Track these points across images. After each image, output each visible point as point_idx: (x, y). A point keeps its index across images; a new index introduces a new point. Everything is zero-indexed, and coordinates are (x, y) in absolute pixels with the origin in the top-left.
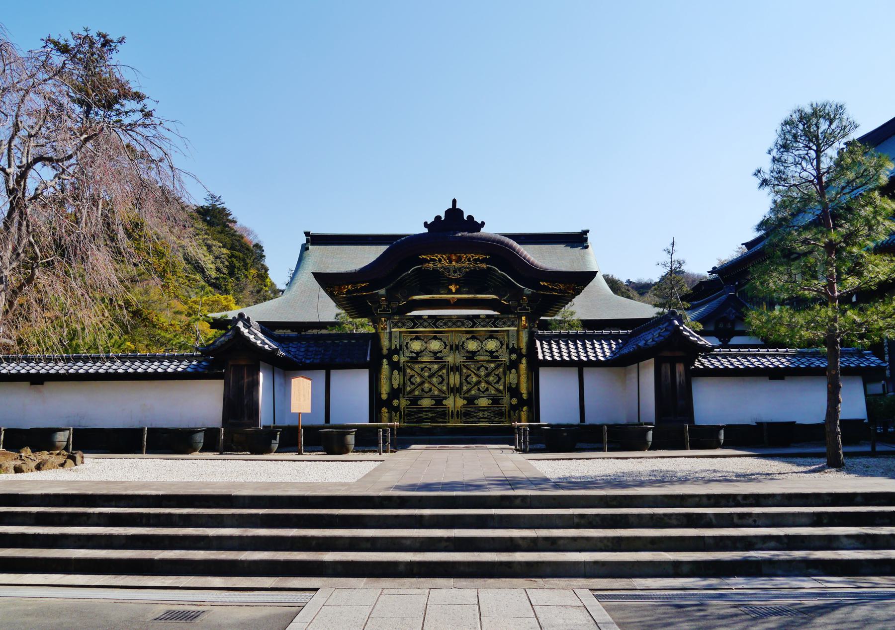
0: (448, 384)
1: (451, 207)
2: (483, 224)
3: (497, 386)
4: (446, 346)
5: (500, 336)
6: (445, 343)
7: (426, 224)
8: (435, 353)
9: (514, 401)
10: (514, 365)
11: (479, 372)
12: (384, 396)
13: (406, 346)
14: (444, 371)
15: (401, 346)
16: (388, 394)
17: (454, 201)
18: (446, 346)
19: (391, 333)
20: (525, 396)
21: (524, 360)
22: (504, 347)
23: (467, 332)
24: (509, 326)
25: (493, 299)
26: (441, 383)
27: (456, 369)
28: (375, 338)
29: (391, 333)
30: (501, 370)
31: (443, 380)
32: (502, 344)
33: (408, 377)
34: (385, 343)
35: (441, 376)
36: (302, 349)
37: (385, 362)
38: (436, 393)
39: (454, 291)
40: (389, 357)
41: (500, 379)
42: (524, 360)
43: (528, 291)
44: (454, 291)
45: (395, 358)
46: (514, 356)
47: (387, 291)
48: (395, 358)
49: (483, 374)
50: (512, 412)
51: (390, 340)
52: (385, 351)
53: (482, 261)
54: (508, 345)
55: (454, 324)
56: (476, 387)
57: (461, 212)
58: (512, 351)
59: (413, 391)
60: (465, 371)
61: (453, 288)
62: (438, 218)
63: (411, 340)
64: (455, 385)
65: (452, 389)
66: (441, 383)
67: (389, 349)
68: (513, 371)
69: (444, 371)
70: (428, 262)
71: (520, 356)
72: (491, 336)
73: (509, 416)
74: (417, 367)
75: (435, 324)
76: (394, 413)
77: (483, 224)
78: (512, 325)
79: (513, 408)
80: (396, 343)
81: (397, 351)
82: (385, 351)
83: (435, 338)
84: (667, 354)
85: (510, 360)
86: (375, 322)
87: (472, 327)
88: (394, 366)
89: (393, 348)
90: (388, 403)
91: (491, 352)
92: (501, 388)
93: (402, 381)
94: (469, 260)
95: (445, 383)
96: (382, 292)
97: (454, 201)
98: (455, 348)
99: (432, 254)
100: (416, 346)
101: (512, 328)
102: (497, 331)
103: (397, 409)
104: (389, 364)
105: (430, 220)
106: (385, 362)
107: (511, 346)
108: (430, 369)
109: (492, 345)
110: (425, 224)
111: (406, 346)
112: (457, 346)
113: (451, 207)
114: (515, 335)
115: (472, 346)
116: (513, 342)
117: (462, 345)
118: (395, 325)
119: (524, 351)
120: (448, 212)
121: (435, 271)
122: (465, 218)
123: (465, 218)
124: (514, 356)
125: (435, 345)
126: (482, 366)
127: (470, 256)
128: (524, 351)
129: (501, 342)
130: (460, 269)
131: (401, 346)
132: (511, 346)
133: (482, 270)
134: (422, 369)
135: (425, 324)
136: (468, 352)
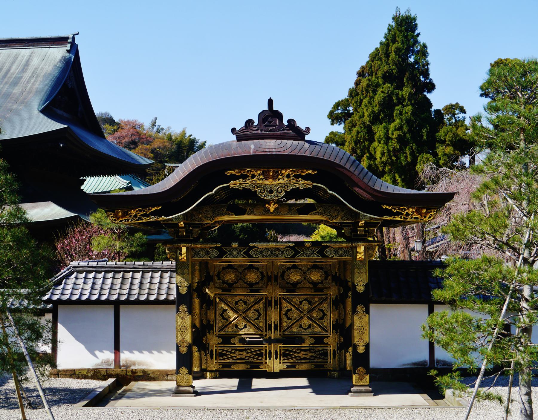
1: (266, 108)
2: (308, 130)
7: (233, 130)
14: (261, 305)
17: (270, 102)
22: (329, 278)
26: (257, 319)
31: (260, 315)
35: (257, 311)
49: (305, 308)
56: (297, 324)
57: (279, 115)
61: (272, 208)
62: (249, 122)
69: (261, 305)
76: (203, 352)
77: (308, 130)
91: (315, 284)
97: (270, 102)
105: (240, 125)
110: (233, 130)
112: (276, 278)
113: (266, 108)
120: (263, 116)
122: (285, 123)
123: (285, 123)
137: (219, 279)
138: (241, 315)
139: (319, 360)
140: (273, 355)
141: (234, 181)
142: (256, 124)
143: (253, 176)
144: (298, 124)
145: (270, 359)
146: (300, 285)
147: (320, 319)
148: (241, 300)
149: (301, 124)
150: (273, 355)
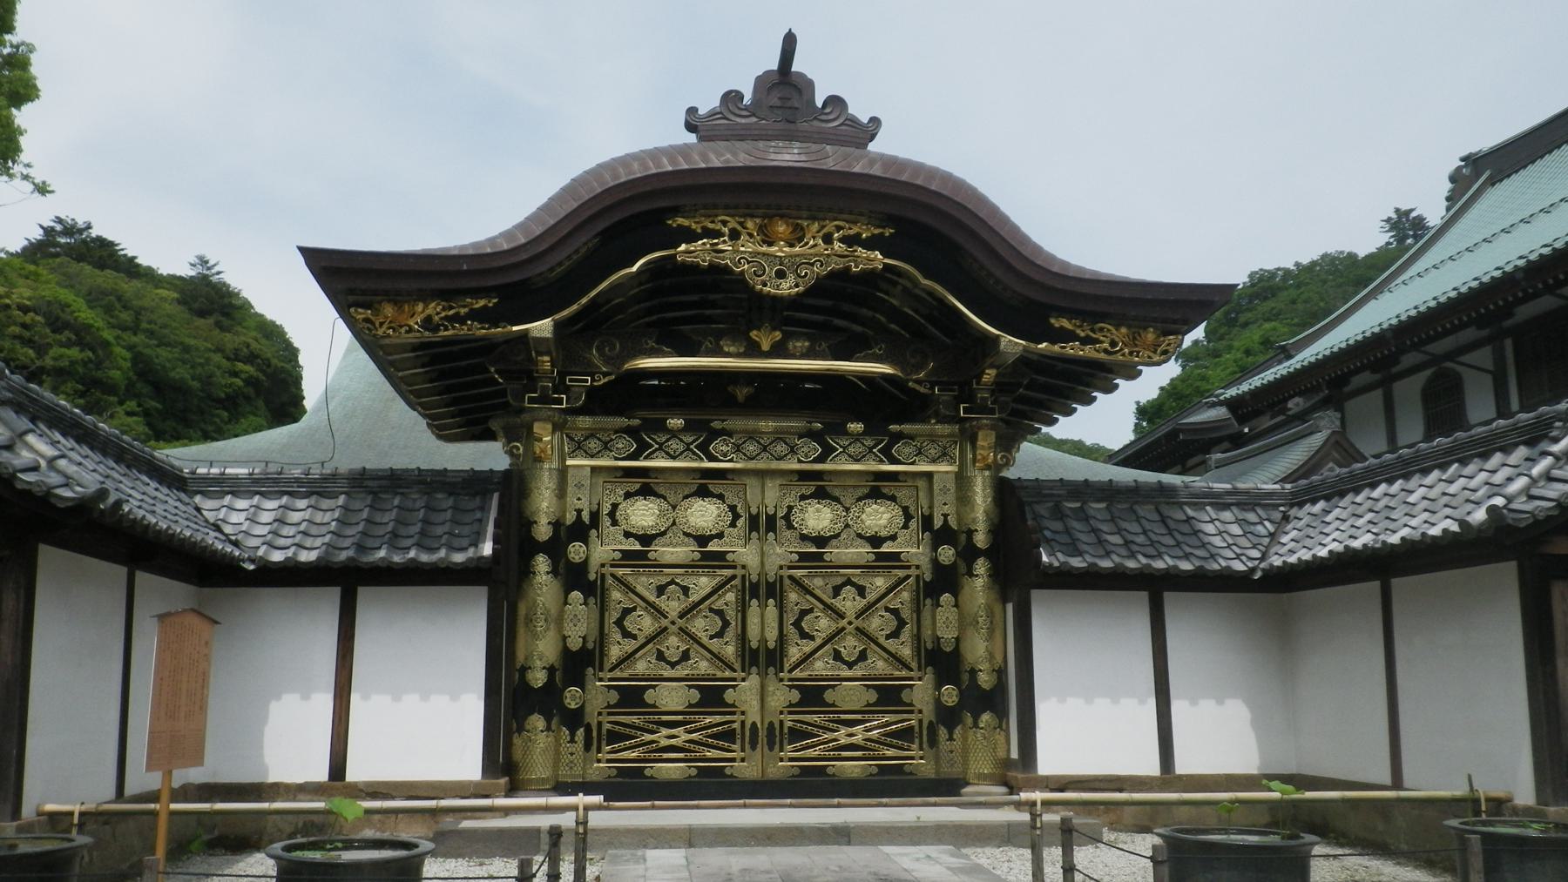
0: (743, 638)
1: (774, 65)
2: (875, 121)
3: (891, 644)
4: (736, 517)
5: (903, 494)
6: (733, 508)
8: (702, 540)
9: (950, 695)
10: (944, 581)
11: (837, 603)
12: (538, 678)
13: (612, 514)
15: (595, 516)
16: (551, 670)
17: (789, 44)
18: (736, 517)
19: (563, 472)
20: (985, 680)
21: (981, 566)
22: (913, 524)
23: (804, 476)
24: (934, 461)
25: (884, 376)
27: (767, 589)
28: (512, 488)
29: (563, 472)
30: (906, 595)
31: (726, 624)
32: (908, 516)
33: (615, 615)
34: (544, 506)
36: (266, 517)
37: (542, 563)
38: (704, 667)
39: (765, 347)
40: (555, 548)
41: (902, 623)
42: (981, 566)
43: (1011, 344)
44: (765, 347)
45: (576, 551)
46: (947, 554)
47: (558, 326)
48: (576, 551)
50: (943, 732)
51: (561, 493)
52: (543, 532)
53: (870, 244)
54: (927, 522)
55: (765, 449)
57: (804, 87)
58: (943, 535)
59: (629, 658)
60: (793, 596)
62: (731, 97)
63: (628, 495)
64: (763, 640)
65: (754, 654)
66: (720, 635)
67: (557, 525)
68: (946, 598)
70: (691, 237)
71: (969, 553)
72: (877, 488)
73: (933, 742)
74: (645, 584)
75: (704, 447)
78: (944, 456)
79: (948, 717)
80: (580, 502)
81: (581, 530)
82: (543, 532)
83: (703, 493)
84: (1565, 546)
85: (935, 562)
86: (512, 435)
87: (821, 459)
88: (574, 577)
89: (570, 518)
90: (547, 701)
92: (906, 652)
93: (595, 625)
94: (828, 239)
95: (730, 634)
96: (542, 327)
97: (789, 44)
98: (763, 525)
99: (712, 217)
100: (644, 514)
101: (943, 467)
102: (893, 476)
103: (574, 719)
104: (554, 572)
105: (708, 103)
106: (542, 563)
107: (938, 523)
108: (686, 590)
109: (878, 517)
111: (612, 514)
114: (952, 486)
115: (818, 517)
116: (944, 509)
117: (787, 517)
118: (579, 448)
119: (981, 539)
121: (718, 272)
124: (947, 554)
125: (704, 514)
126: (849, 582)
127: (830, 227)
128: (981, 539)
129: (905, 510)
130: (796, 265)
131: (595, 516)
132: (938, 523)
133: (869, 276)
134: (661, 590)
135: (675, 445)
136: (804, 538)
137: (615, 523)
138: (673, 623)
139: (889, 753)
140: (762, 734)
141: (688, 242)
142: (747, 99)
143: (735, 235)
144: (852, 110)
145: (754, 748)
146: (834, 542)
147: (888, 637)
148: (672, 582)
149: (860, 111)
150: (762, 734)
